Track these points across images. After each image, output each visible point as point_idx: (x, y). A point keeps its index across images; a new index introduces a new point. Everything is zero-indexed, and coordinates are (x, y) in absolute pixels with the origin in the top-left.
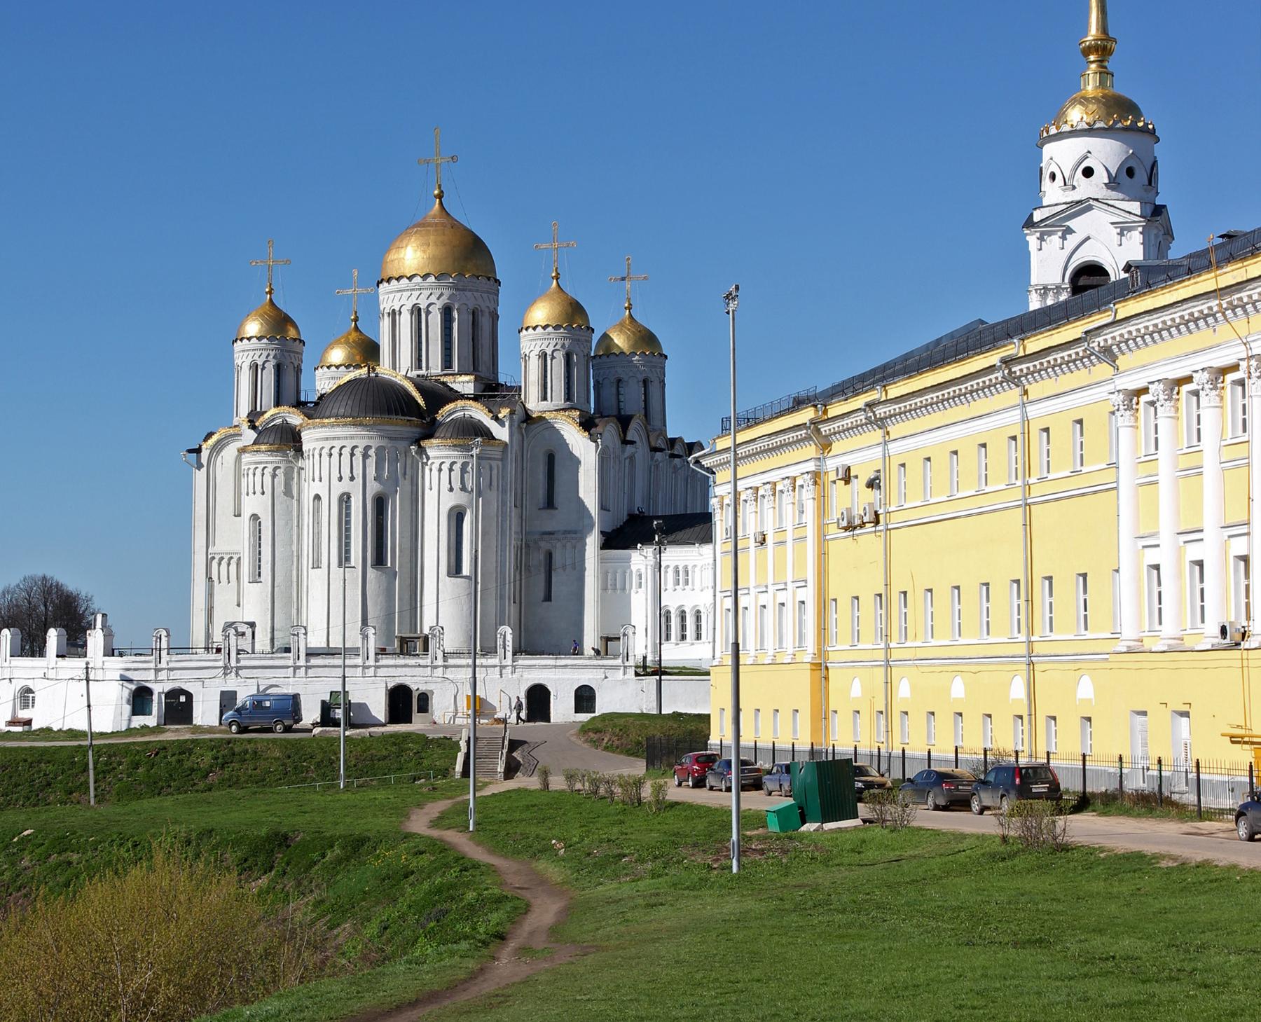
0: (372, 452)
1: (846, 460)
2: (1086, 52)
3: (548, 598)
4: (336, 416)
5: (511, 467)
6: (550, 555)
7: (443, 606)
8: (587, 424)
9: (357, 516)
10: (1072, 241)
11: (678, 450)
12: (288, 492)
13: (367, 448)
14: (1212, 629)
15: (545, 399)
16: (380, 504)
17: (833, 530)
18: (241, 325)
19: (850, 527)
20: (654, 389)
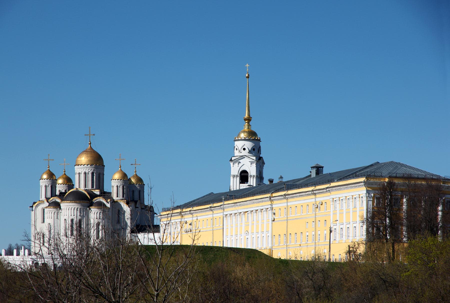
0: (79, 209)
1: (185, 220)
2: (245, 120)
4: (70, 200)
8: (127, 203)
12: (57, 218)
13: (78, 208)
15: (118, 197)
17: (183, 232)
18: (42, 176)
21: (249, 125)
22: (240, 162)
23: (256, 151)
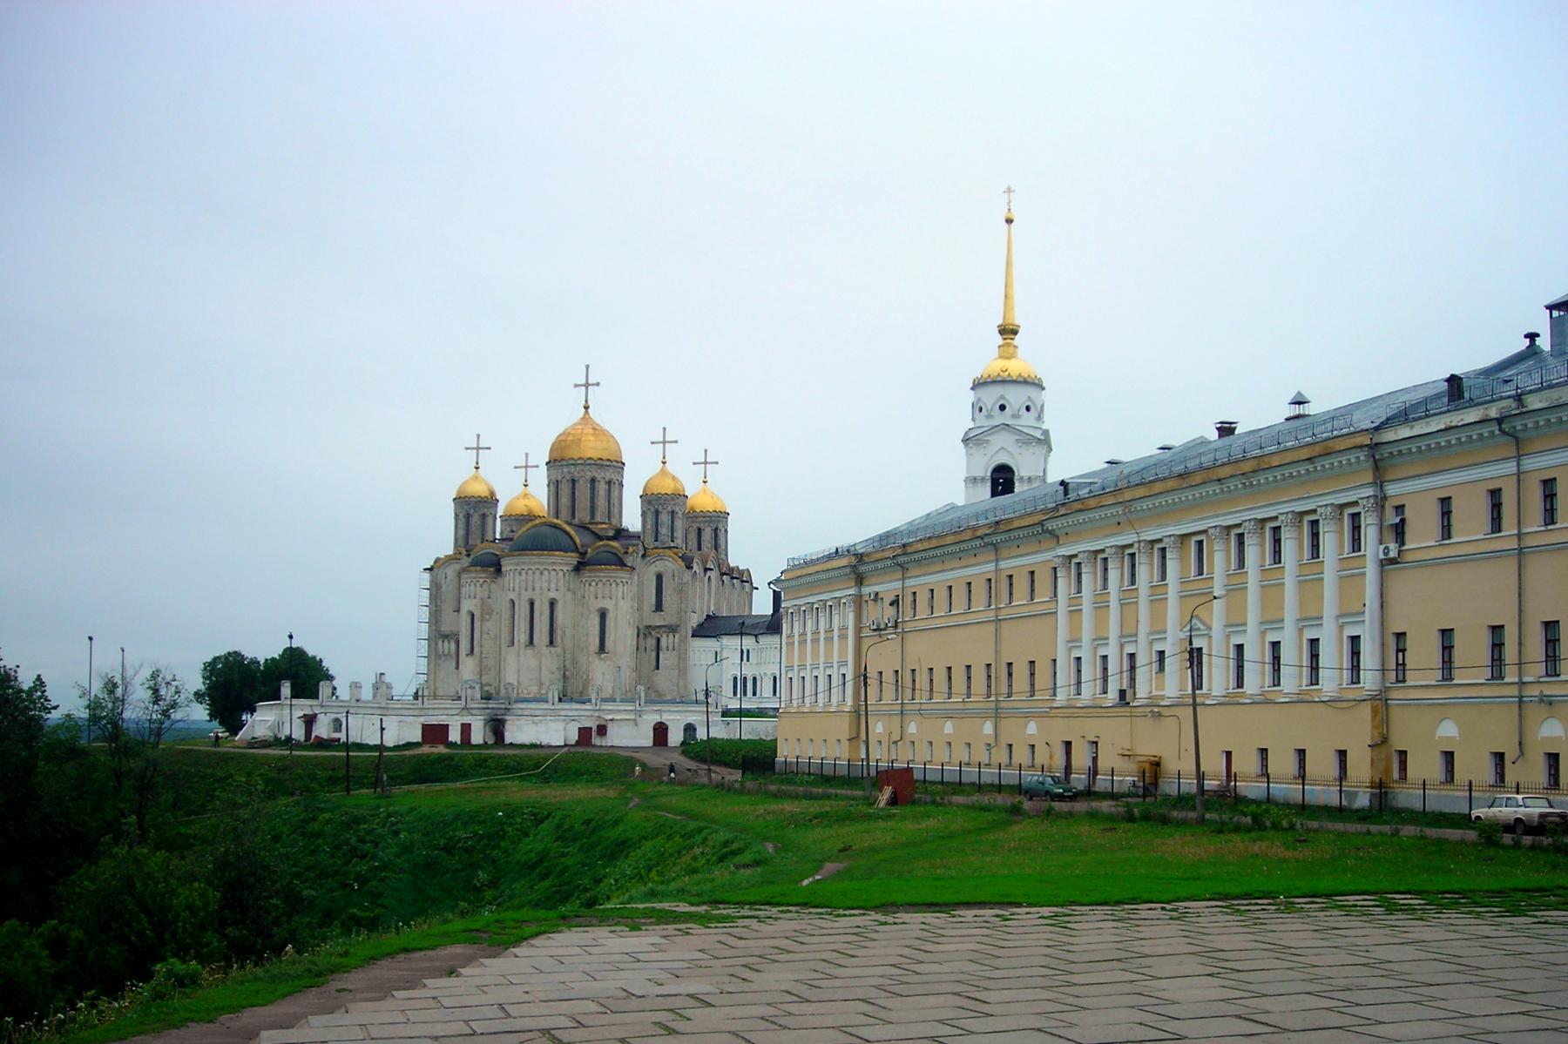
1: (876, 589)
3: (658, 668)
6: (658, 640)
10: (992, 449)
14: (1113, 695)
16: (552, 604)
19: (878, 629)
20: (721, 535)
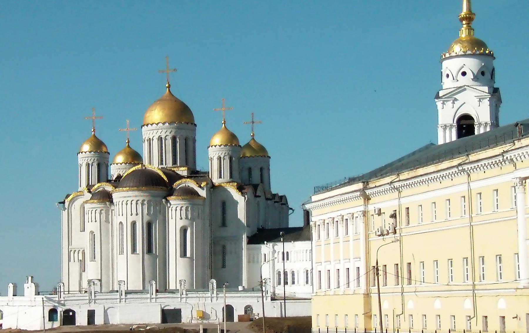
0: (146, 202)
1: (378, 206)
3: (224, 266)
4: (129, 187)
5: (207, 209)
6: (224, 247)
7: (178, 270)
8: (240, 189)
9: (139, 231)
11: (277, 199)
12: (107, 221)
13: (143, 201)
15: (220, 177)
18: (81, 146)
19: (382, 235)
21: (470, 28)
22: (456, 100)
23: (486, 75)
